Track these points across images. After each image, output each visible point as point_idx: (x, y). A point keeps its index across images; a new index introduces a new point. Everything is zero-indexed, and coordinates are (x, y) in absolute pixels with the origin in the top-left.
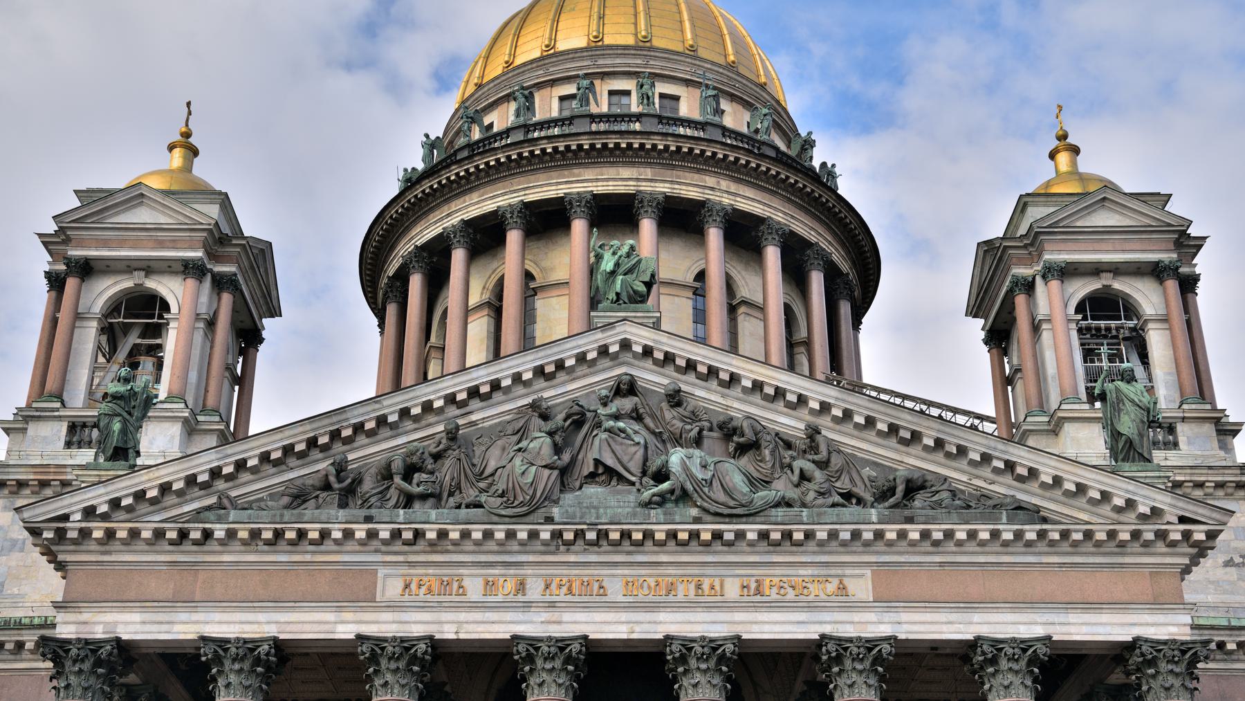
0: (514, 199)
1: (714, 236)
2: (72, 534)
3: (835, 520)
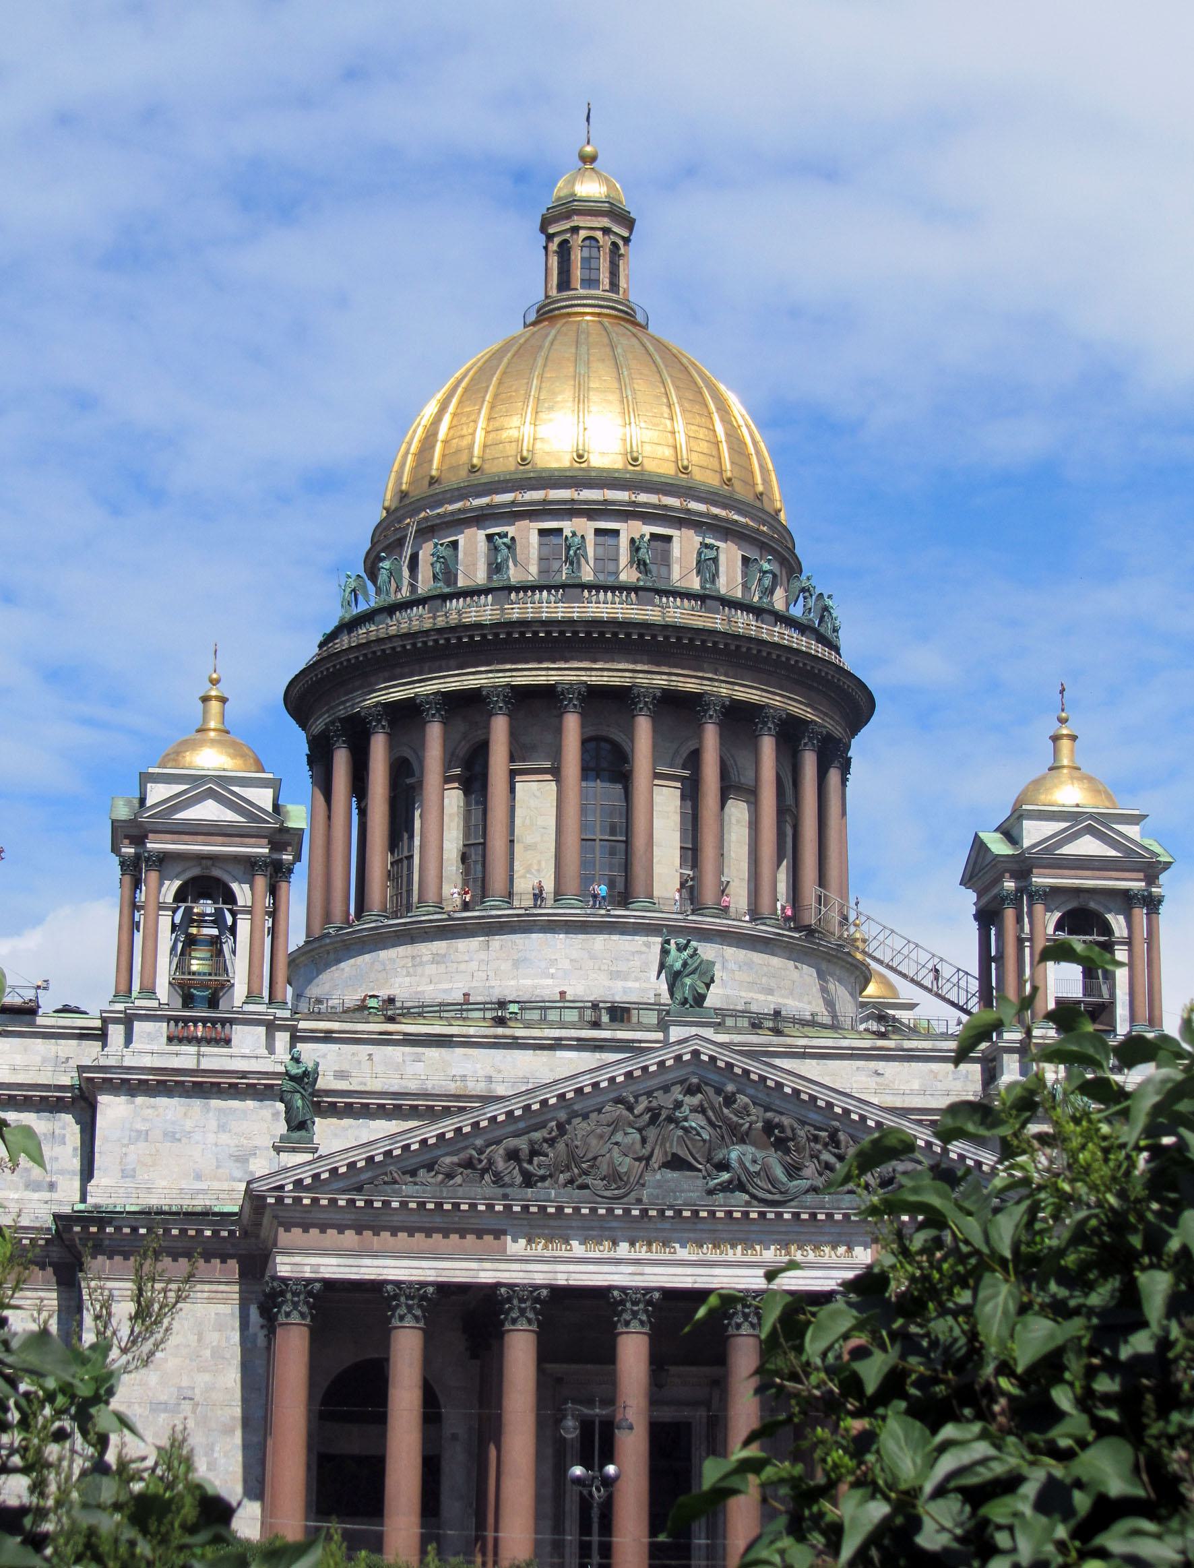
0: (502, 679)
1: (711, 737)
2: (288, 1201)
3: (848, 1205)
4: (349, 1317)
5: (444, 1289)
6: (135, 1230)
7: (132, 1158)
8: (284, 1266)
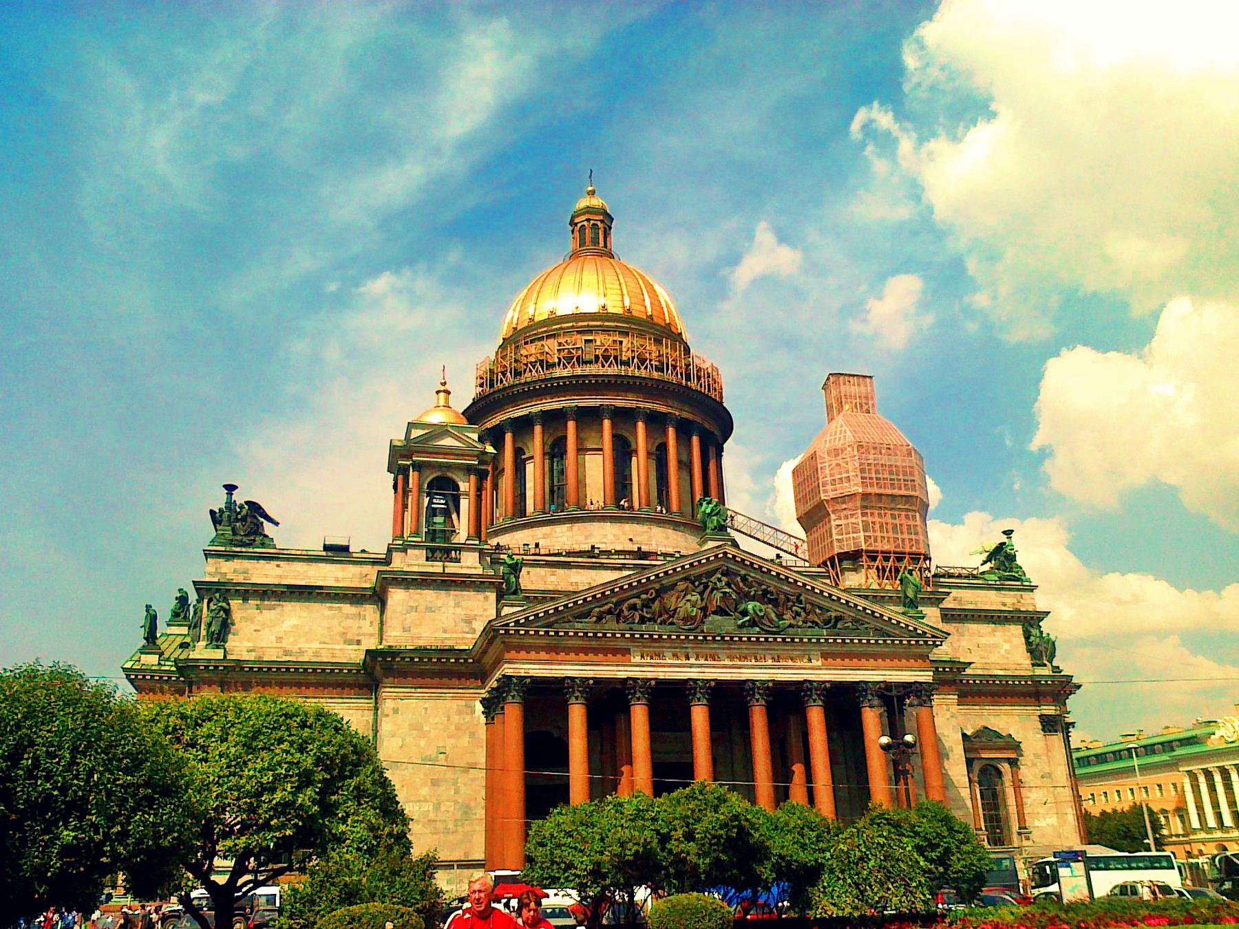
1: (671, 432)
4: (544, 700)
5: (597, 681)
6: (412, 659)
7: (408, 621)
8: (508, 669)
